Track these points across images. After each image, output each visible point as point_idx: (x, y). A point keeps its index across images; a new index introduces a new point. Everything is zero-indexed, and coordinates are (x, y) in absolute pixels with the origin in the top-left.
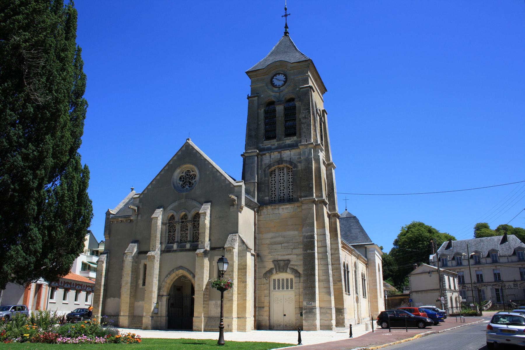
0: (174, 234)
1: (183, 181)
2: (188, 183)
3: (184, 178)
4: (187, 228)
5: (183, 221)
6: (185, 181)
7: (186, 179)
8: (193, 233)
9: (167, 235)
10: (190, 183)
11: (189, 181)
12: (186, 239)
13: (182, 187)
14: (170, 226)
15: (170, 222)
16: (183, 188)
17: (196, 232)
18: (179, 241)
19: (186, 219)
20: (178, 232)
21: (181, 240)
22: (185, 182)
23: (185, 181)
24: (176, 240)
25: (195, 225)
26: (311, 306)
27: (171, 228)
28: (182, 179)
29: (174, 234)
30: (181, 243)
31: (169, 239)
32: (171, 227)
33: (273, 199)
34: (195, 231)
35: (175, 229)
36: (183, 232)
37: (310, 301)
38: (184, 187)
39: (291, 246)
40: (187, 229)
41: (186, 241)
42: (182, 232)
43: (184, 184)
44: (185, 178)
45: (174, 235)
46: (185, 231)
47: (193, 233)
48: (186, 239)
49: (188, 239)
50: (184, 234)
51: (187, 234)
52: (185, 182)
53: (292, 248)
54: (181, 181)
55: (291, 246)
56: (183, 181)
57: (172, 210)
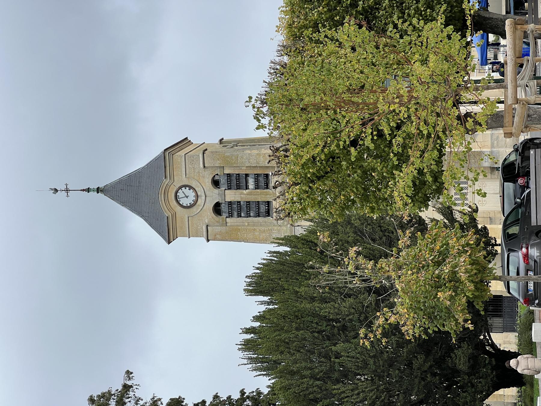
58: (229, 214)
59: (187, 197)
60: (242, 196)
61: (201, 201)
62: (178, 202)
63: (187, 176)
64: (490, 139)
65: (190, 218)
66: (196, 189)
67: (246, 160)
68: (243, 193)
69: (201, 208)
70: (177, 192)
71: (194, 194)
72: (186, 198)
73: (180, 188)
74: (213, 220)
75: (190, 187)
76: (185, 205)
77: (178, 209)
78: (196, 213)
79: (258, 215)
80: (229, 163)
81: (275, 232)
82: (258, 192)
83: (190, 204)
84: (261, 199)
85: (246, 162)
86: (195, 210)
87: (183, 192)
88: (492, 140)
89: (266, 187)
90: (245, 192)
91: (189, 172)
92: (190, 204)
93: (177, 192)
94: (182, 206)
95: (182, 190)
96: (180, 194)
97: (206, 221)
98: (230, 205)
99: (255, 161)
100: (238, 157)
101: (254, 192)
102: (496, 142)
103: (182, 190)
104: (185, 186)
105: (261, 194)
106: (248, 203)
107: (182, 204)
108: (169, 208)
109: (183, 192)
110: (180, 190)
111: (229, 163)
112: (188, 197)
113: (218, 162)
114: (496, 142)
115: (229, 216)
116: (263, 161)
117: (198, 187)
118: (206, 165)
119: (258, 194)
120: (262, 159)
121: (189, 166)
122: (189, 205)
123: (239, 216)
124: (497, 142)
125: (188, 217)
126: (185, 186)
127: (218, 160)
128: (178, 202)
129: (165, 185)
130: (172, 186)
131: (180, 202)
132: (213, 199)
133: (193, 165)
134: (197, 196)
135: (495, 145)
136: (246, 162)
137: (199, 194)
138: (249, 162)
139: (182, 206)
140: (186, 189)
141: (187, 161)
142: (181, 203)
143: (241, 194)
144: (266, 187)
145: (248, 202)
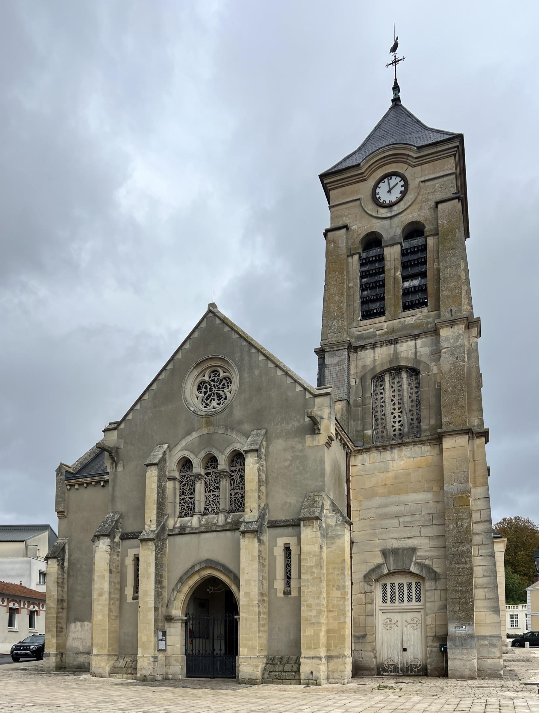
0: (191, 498)
1: (205, 393)
2: (215, 397)
3: (206, 388)
4: (217, 485)
5: (209, 471)
6: (208, 393)
7: (210, 388)
8: (231, 494)
9: (178, 501)
10: (219, 396)
11: (217, 393)
12: (215, 506)
13: (204, 405)
14: (183, 482)
15: (183, 474)
16: (205, 407)
17: (236, 491)
18: (203, 510)
19: (214, 468)
20: (200, 493)
21: (205, 508)
22: (209, 396)
23: (208, 393)
24: (197, 510)
25: (232, 479)
26: (463, 633)
27: (185, 487)
28: (204, 390)
29: (191, 498)
30: (205, 514)
31: (182, 508)
32: (184, 485)
33: (380, 434)
34: (234, 490)
35: (194, 489)
36: (210, 494)
37: (463, 625)
38: (207, 404)
39: (418, 521)
40: (218, 488)
41: (216, 510)
42: (207, 494)
43: (207, 399)
44: (209, 387)
45: (191, 500)
46: (213, 491)
47: (231, 494)
48: (215, 506)
49: (222, 506)
50: (212, 497)
51: (218, 496)
52: (209, 396)
53: (421, 524)
54: (201, 393)
55: (418, 521)
56: (205, 393)
57: (186, 450)
58: (365, 259)
59: (389, 191)
60: (393, 271)
61: (383, 212)
62: (381, 180)
63: (422, 184)
64: (491, 634)
65: (358, 202)
66: (402, 203)
67: (449, 263)
68: (397, 271)
69: (374, 214)
70: (396, 174)
71: (394, 199)
72: (388, 189)
73: (403, 178)
74: (356, 235)
75: (404, 193)
76: (377, 191)
77: (371, 182)
78: (366, 209)
79: (364, 301)
80: (445, 239)
81: (340, 324)
82: (399, 292)
83: (380, 198)
84: (388, 299)
85: (447, 263)
86: (370, 208)
87: (397, 183)
88: (490, 637)
89: (407, 304)
90: (399, 274)
91: (428, 186)
92: (380, 198)
93: (396, 174)
94: (376, 186)
95: (400, 181)
96: (394, 180)
97: (354, 227)
98: (379, 257)
99: (448, 276)
100: (454, 250)
101: (398, 287)
102: (486, 642)
103: (400, 181)
104: (406, 185)
105: (396, 297)
106: (382, 284)
107: (379, 186)
108: (372, 167)
109: (397, 183)
110: (400, 179)
111: (445, 239)
112: (389, 193)
113: (445, 222)
114: (486, 642)
115: (362, 259)
116: (447, 288)
117: (405, 204)
118: (440, 206)
119: (396, 293)
120: (452, 285)
121: (438, 183)
122: (378, 196)
123: (363, 275)
124: (486, 645)
125: (359, 199)
126: (406, 185)
127: (448, 222)
128: (381, 180)
129: (407, 152)
130: (406, 166)
131: (381, 183)
132: (387, 229)
133: (440, 189)
134: (391, 206)
135: (482, 642)
136: (447, 263)
137: (395, 208)
138: (445, 267)
139: (376, 186)
140: (402, 186)
141: (445, 179)
142: (381, 185)
143: (396, 269)
144: (407, 304)
145: (383, 282)
